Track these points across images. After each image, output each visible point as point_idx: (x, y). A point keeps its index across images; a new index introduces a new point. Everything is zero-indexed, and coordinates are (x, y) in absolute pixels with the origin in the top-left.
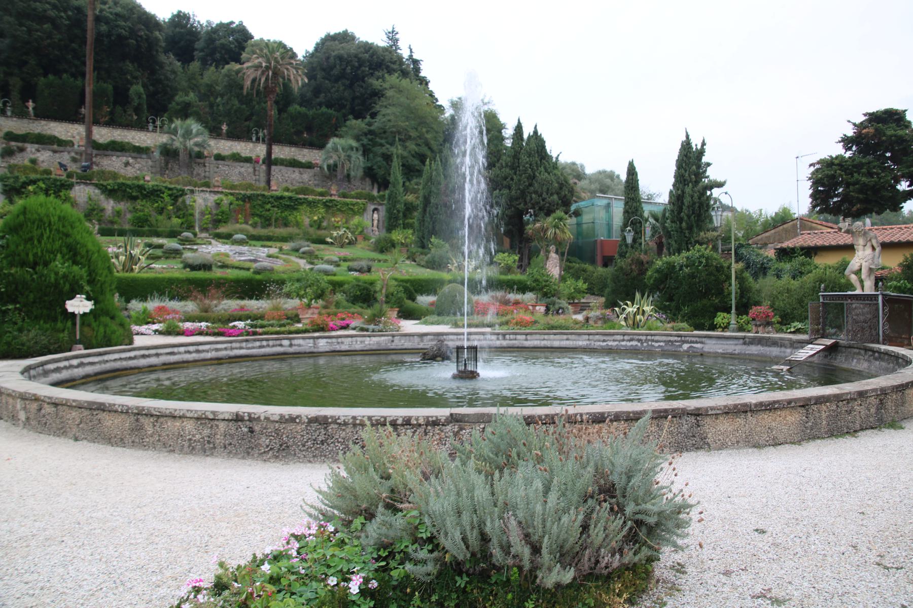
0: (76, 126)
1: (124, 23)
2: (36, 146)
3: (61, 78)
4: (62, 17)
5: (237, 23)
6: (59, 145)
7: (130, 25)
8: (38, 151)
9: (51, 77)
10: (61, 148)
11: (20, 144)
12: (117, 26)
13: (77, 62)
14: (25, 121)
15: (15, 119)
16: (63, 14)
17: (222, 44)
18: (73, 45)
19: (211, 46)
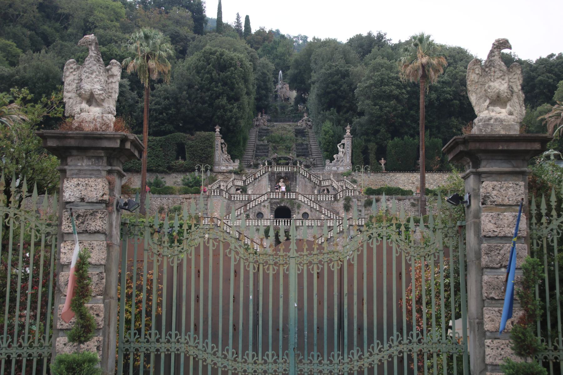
0: (415, 174)
1: (449, 89)
2: (387, 196)
3: (403, 139)
4: (403, 93)
5: (557, 55)
6: (402, 195)
7: (454, 89)
8: (388, 200)
9: (396, 139)
10: (404, 197)
11: (377, 197)
12: (444, 92)
13: (414, 125)
14: (379, 174)
15: (372, 174)
16: (404, 91)
17: (541, 81)
18: (412, 112)
19: (531, 83)
